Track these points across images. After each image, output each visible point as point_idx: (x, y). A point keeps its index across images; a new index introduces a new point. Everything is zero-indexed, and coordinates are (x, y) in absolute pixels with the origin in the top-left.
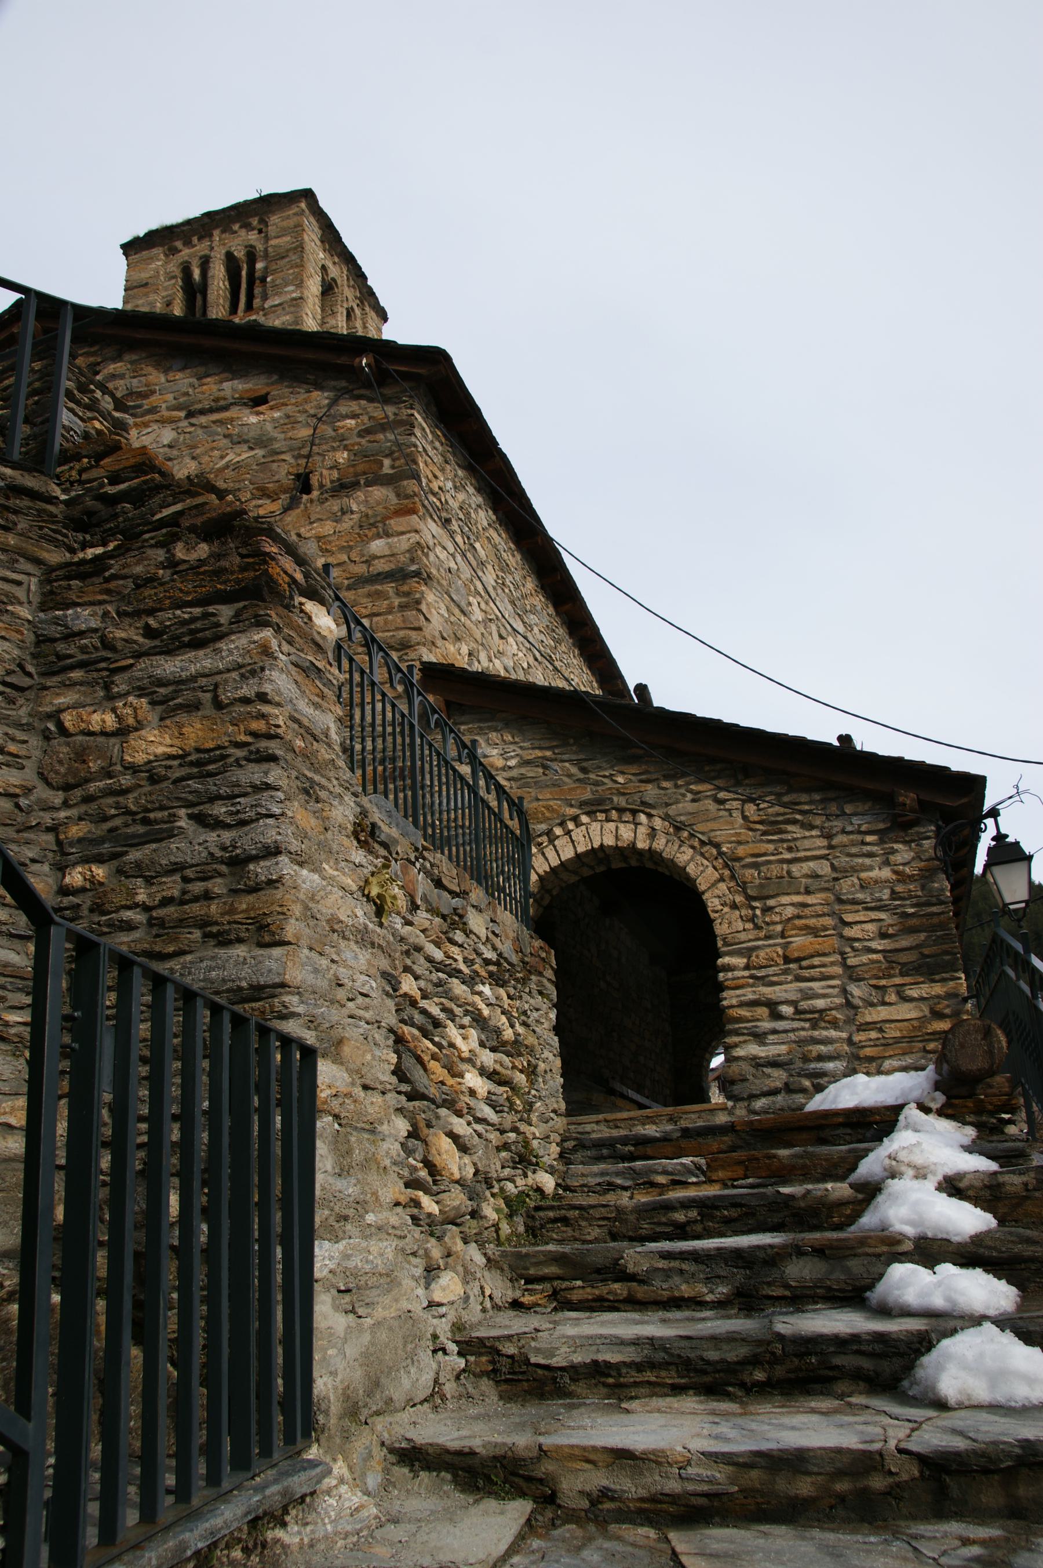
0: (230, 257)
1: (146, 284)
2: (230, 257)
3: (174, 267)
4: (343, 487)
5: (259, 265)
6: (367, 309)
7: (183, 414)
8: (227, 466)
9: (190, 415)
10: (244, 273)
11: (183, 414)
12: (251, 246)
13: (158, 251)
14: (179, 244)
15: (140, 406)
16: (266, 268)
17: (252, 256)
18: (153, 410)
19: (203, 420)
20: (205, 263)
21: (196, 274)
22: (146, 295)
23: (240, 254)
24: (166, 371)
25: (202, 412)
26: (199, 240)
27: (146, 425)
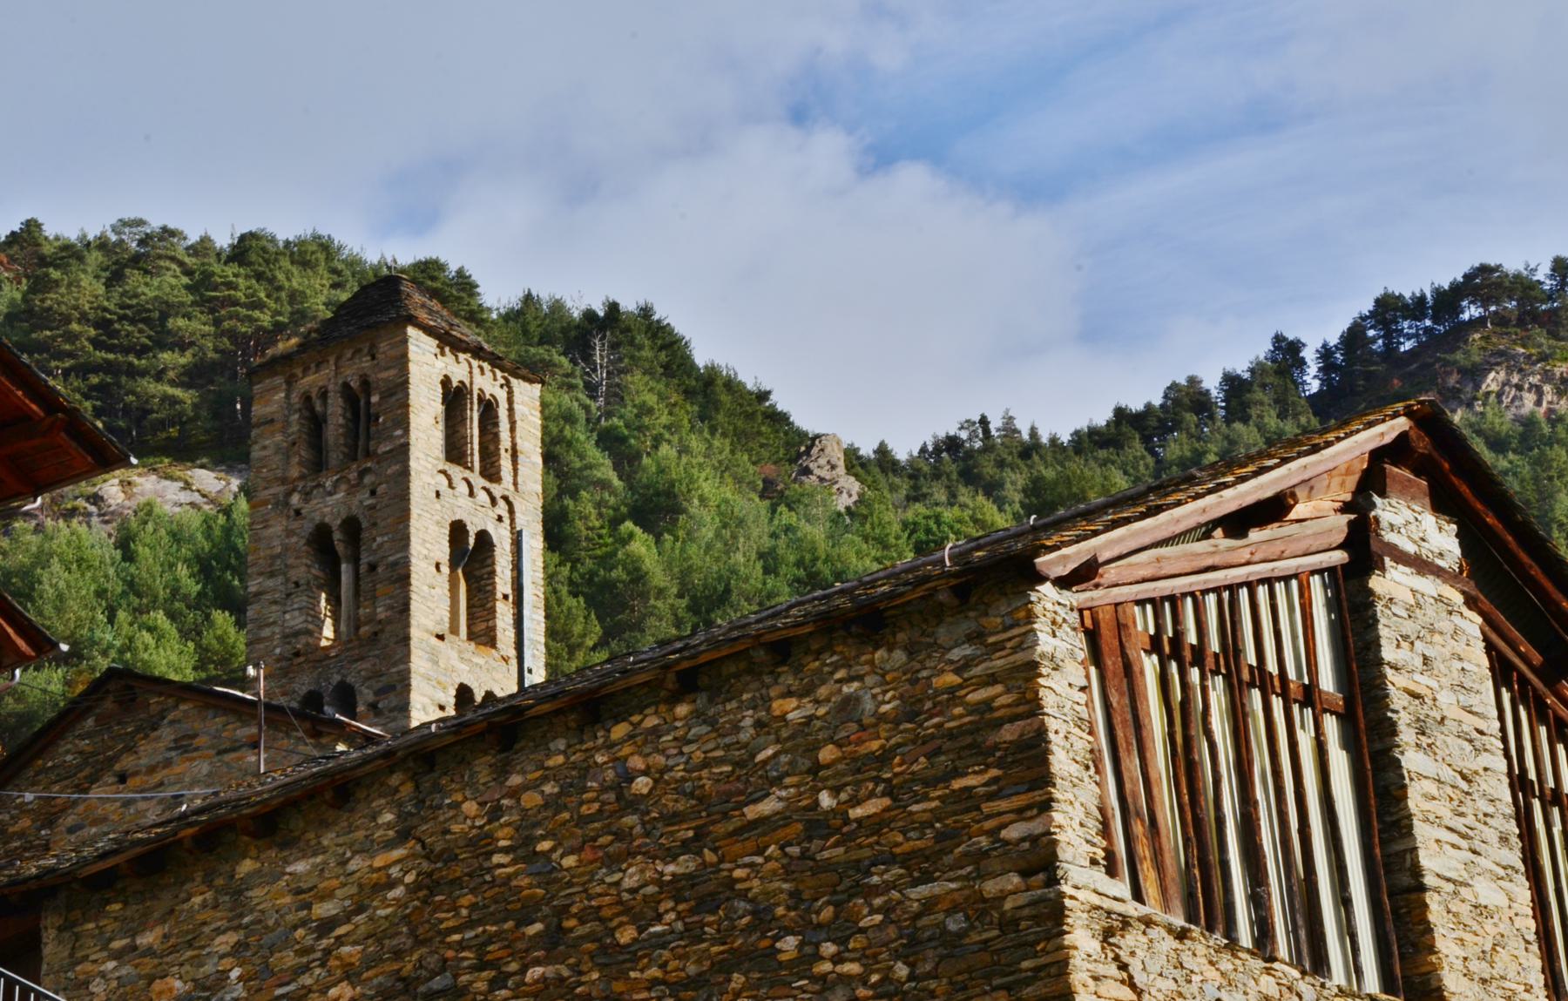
1: (272, 421)
3: (295, 398)
5: (375, 399)
6: (514, 381)
7: (213, 752)
9: (219, 753)
10: (362, 403)
11: (213, 752)
13: (279, 380)
14: (298, 371)
16: (379, 404)
17: (366, 384)
19: (227, 757)
20: (324, 395)
21: (318, 408)
22: (273, 434)
24: (204, 719)
25: (226, 751)
26: (317, 366)
27: (194, 759)
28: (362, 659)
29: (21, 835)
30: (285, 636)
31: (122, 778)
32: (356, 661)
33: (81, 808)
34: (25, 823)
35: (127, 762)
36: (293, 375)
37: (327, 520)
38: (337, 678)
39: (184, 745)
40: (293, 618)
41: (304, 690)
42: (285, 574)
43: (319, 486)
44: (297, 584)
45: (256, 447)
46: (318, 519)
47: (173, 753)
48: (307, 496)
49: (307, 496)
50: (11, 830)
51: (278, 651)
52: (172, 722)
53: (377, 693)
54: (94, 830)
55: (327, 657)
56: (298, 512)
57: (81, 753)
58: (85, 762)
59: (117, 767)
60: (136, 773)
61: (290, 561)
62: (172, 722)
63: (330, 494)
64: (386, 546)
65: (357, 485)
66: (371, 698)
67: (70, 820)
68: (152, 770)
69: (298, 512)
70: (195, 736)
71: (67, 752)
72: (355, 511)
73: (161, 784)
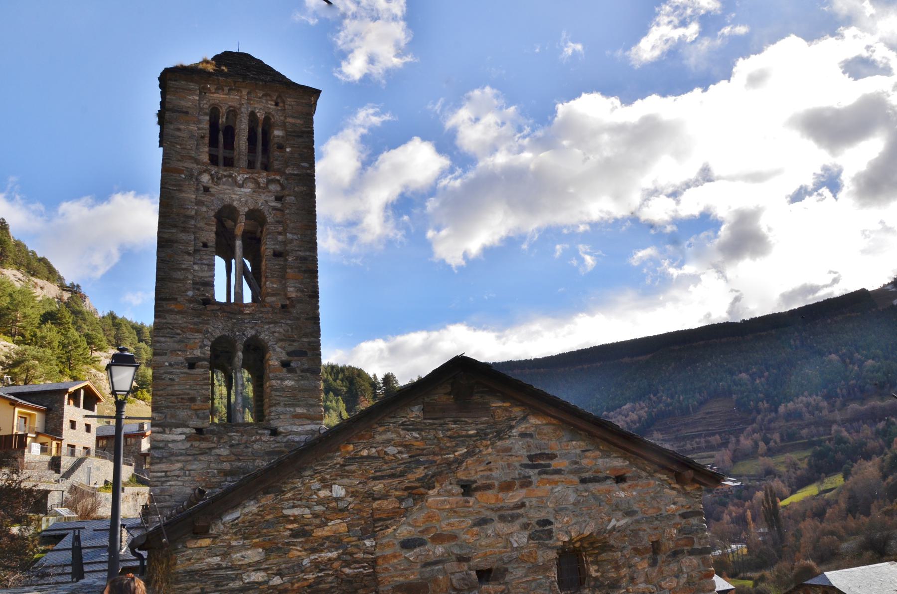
0: (252, 115)
2: (252, 115)
3: (205, 105)
4: (676, 554)
8: (614, 528)
9: (583, 481)
12: (270, 113)
15: (549, 465)
18: (558, 472)
23: (260, 115)
27: (556, 483)
28: (275, 323)
29: (336, 541)
30: (195, 283)
31: (467, 489)
32: (269, 323)
33: (419, 516)
34: (337, 526)
35: (473, 471)
36: (205, 88)
37: (235, 204)
38: (250, 333)
39: (540, 462)
40: (203, 271)
41: (218, 334)
42: (194, 233)
43: (230, 176)
44: (205, 245)
45: (172, 127)
46: (227, 201)
47: (531, 472)
48: (216, 180)
49: (216, 180)
50: (319, 533)
51: (190, 293)
52: (523, 435)
53: (289, 354)
54: (440, 550)
55: (241, 312)
56: (206, 190)
57: (407, 447)
58: (414, 461)
59: (461, 475)
60: (488, 487)
61: (201, 224)
62: (523, 435)
63: (241, 186)
64: (295, 243)
65: (264, 188)
66: (284, 357)
67: (404, 531)
68: (507, 487)
69: (206, 190)
70: (552, 457)
71: (388, 442)
72: (260, 205)
73: (523, 505)
